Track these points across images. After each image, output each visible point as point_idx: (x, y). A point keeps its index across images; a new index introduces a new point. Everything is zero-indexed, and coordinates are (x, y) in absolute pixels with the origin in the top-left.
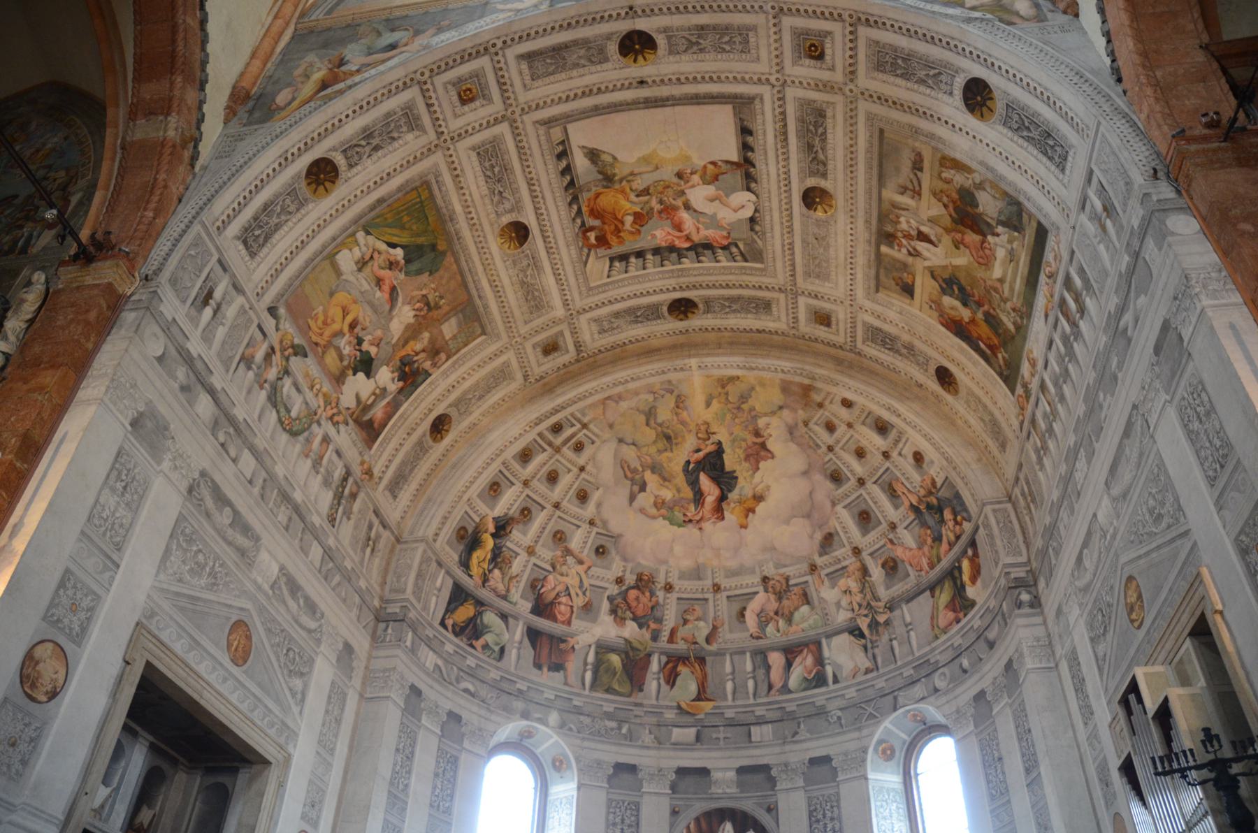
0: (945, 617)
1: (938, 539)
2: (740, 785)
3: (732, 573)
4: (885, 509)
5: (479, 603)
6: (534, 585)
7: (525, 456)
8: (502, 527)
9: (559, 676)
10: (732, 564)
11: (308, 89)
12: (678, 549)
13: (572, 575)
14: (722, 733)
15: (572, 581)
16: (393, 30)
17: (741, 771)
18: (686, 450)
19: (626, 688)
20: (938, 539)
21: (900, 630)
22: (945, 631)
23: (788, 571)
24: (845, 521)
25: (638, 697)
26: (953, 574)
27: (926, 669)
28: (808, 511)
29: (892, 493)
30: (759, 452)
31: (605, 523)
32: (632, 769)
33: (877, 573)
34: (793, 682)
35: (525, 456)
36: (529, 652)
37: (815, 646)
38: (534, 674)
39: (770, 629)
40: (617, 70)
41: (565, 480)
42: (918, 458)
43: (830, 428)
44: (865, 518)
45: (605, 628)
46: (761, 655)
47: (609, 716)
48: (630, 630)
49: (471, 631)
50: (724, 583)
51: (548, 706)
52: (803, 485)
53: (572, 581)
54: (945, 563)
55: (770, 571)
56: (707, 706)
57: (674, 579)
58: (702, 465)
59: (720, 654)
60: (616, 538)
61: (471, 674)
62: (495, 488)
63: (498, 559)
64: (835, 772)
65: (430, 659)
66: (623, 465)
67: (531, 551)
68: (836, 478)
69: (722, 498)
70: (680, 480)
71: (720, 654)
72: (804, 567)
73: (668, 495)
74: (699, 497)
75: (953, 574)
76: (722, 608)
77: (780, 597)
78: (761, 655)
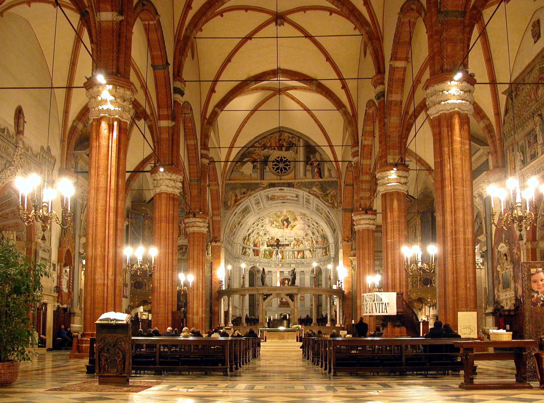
0: (324, 254)
1: (324, 242)
5: (246, 248)
6: (253, 242)
7: (254, 224)
8: (249, 235)
9: (258, 257)
10: (289, 236)
11: (233, 202)
12: (279, 233)
16: (243, 188)
18: (282, 218)
19: (269, 257)
20: (324, 242)
21: (317, 253)
22: (324, 256)
23: (299, 238)
24: (310, 233)
25: (271, 259)
26: (326, 248)
30: (295, 219)
31: (266, 230)
32: (271, 272)
33: (314, 242)
35: (254, 224)
39: (295, 247)
40: (278, 191)
42: (322, 230)
43: (308, 220)
44: (313, 233)
46: (293, 252)
47: (267, 263)
49: (244, 253)
51: (256, 262)
52: (303, 226)
54: (325, 246)
55: (296, 237)
56: (284, 260)
58: (284, 220)
59: (286, 251)
60: (268, 232)
62: (249, 230)
64: (304, 274)
66: (270, 221)
67: (253, 237)
68: (309, 226)
69: (288, 225)
70: (280, 222)
71: (286, 251)
72: (302, 238)
73: (278, 224)
74: (284, 225)
75: (326, 248)
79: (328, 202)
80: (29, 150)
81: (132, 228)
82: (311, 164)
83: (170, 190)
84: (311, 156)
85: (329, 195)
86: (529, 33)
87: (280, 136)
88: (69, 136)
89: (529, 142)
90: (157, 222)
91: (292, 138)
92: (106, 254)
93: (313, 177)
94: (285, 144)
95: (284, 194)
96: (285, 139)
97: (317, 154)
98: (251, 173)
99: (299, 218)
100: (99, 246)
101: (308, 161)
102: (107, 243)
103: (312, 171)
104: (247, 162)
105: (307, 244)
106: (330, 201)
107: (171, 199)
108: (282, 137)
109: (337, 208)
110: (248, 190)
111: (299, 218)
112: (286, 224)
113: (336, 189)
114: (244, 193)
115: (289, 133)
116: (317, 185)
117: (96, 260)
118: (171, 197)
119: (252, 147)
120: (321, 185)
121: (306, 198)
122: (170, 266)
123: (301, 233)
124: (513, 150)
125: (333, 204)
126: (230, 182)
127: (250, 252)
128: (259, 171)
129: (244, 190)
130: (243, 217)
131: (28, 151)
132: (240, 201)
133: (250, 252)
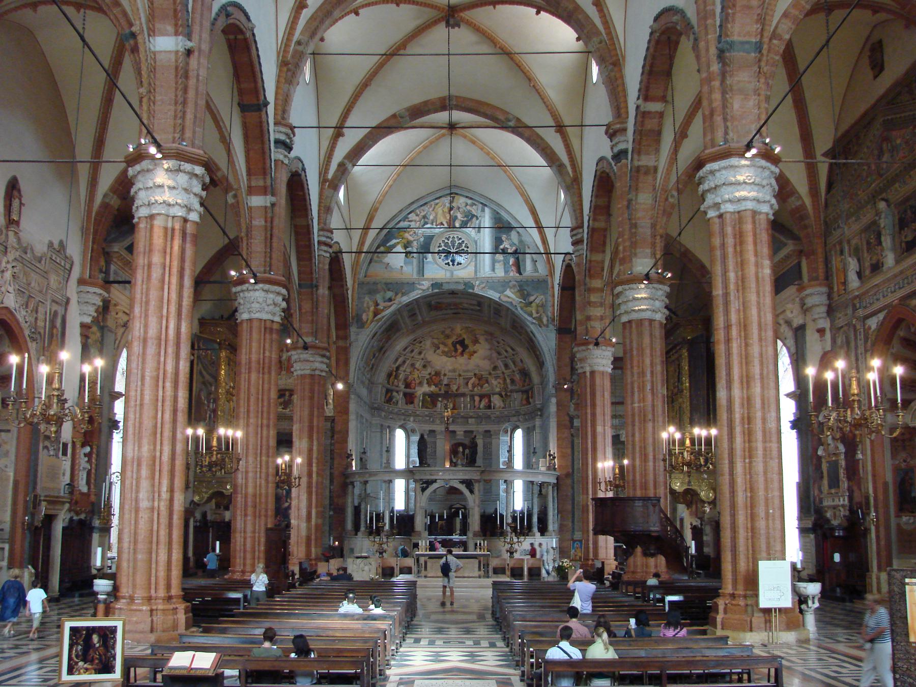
0: (524, 402)
2: (465, 437)
3: (465, 371)
4: (511, 365)
6: (405, 380)
7: (406, 348)
8: (398, 368)
11: (371, 315)
12: (449, 364)
13: (416, 374)
14: (460, 420)
15: (416, 376)
16: (389, 290)
17: (465, 432)
18: (454, 338)
20: (525, 381)
24: (500, 364)
26: (526, 392)
27: (518, 414)
28: (490, 358)
29: (514, 363)
30: (476, 341)
33: (508, 381)
34: (482, 406)
35: (405, 349)
36: (404, 401)
37: (488, 396)
38: (406, 407)
41: (416, 351)
43: (498, 343)
44: (506, 366)
45: (426, 389)
46: (472, 397)
48: (433, 388)
49: (389, 400)
50: (462, 374)
51: (410, 415)
53: (416, 376)
55: (477, 372)
57: (447, 372)
58: (457, 343)
61: (391, 413)
62: (397, 360)
63: (396, 377)
64: (491, 435)
65: (383, 414)
66: (433, 343)
68: (499, 353)
69: (463, 351)
70: (451, 346)
73: (446, 349)
74: (456, 350)
76: (461, 381)
77: (480, 379)
78: (472, 397)
79: (531, 315)
80: (29, 251)
81: (200, 365)
82: (504, 252)
83: (265, 316)
84: (504, 237)
85: (534, 305)
86: (865, 61)
87: (451, 202)
88: (95, 219)
89: (868, 243)
90: (243, 370)
91: (473, 204)
92: (158, 454)
93: (506, 272)
94: (459, 216)
95: (458, 301)
96: (459, 208)
97: (513, 234)
98: (402, 264)
99: (482, 339)
100: (145, 441)
101: (497, 250)
102: (159, 436)
103: (506, 263)
104: (394, 246)
105: (496, 384)
106: (535, 315)
107: (268, 331)
108: (454, 205)
109: (547, 326)
110: (396, 294)
111: (482, 339)
112: (460, 349)
113: (545, 294)
114: (390, 300)
115: (467, 197)
116: (514, 286)
117: (139, 465)
118: (266, 327)
119: (405, 218)
120: (520, 286)
121: (495, 308)
122: (264, 447)
123: (486, 365)
124: (842, 252)
125: (539, 319)
126: (367, 279)
127: (399, 397)
128: (415, 261)
129: (389, 294)
130: (389, 339)
131: (26, 253)
132: (383, 314)
133: (399, 397)
